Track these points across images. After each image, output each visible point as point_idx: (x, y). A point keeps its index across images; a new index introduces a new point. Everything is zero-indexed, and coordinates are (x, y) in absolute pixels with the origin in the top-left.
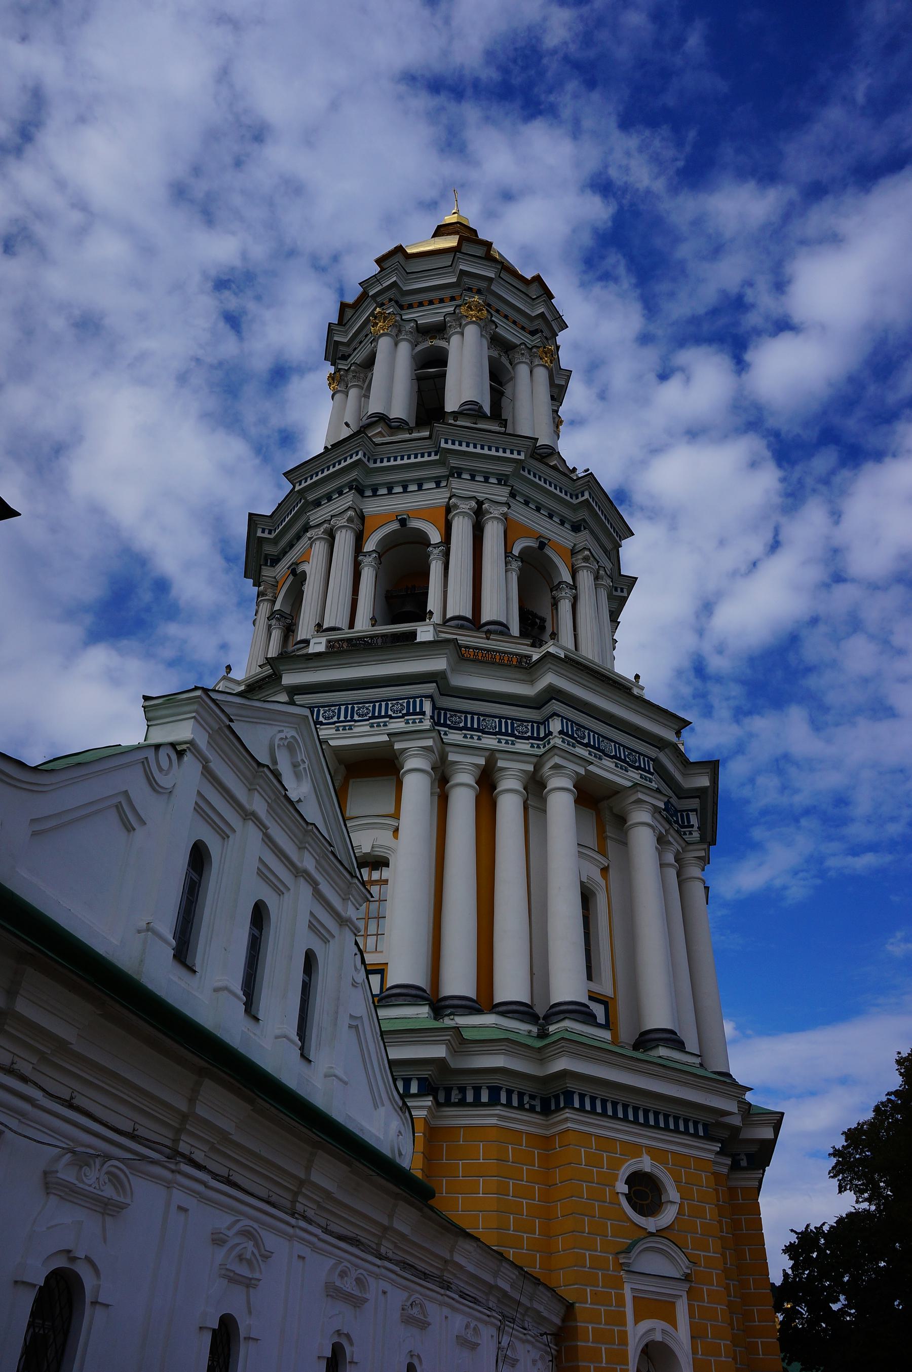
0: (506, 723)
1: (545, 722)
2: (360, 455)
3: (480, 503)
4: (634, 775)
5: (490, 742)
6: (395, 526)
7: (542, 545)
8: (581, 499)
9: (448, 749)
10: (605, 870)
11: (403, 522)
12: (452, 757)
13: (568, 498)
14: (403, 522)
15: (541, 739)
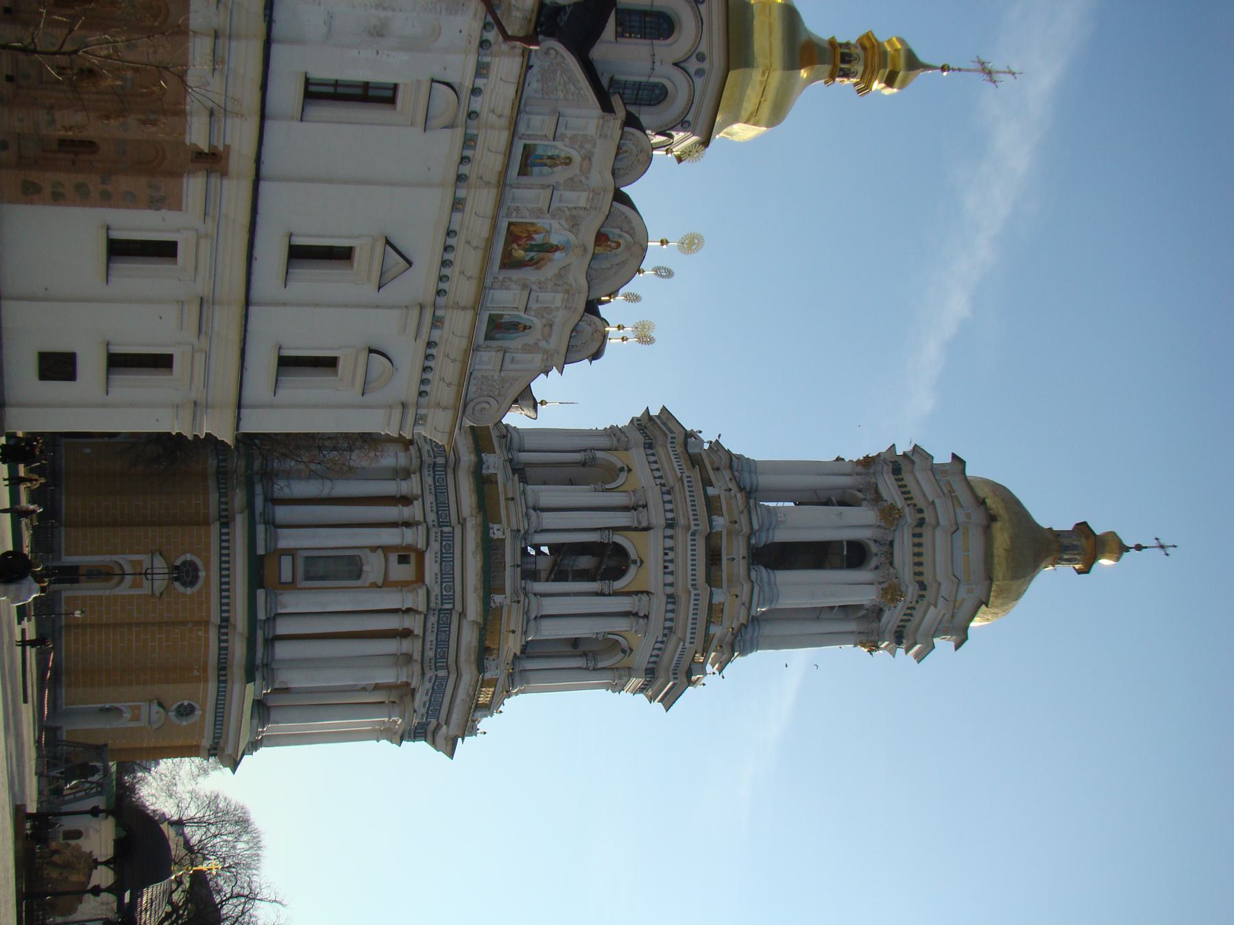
0: (446, 507)
1: (450, 526)
2: (670, 435)
3: (645, 506)
4: (436, 590)
5: (430, 499)
6: (620, 465)
7: (635, 562)
8: (692, 590)
9: (418, 474)
10: (374, 585)
11: (622, 469)
12: (412, 475)
13: (690, 582)
14: (622, 469)
15: (439, 525)
